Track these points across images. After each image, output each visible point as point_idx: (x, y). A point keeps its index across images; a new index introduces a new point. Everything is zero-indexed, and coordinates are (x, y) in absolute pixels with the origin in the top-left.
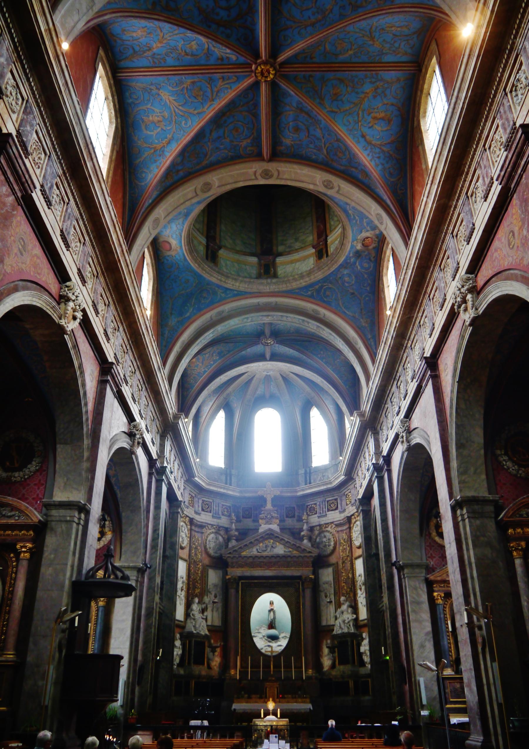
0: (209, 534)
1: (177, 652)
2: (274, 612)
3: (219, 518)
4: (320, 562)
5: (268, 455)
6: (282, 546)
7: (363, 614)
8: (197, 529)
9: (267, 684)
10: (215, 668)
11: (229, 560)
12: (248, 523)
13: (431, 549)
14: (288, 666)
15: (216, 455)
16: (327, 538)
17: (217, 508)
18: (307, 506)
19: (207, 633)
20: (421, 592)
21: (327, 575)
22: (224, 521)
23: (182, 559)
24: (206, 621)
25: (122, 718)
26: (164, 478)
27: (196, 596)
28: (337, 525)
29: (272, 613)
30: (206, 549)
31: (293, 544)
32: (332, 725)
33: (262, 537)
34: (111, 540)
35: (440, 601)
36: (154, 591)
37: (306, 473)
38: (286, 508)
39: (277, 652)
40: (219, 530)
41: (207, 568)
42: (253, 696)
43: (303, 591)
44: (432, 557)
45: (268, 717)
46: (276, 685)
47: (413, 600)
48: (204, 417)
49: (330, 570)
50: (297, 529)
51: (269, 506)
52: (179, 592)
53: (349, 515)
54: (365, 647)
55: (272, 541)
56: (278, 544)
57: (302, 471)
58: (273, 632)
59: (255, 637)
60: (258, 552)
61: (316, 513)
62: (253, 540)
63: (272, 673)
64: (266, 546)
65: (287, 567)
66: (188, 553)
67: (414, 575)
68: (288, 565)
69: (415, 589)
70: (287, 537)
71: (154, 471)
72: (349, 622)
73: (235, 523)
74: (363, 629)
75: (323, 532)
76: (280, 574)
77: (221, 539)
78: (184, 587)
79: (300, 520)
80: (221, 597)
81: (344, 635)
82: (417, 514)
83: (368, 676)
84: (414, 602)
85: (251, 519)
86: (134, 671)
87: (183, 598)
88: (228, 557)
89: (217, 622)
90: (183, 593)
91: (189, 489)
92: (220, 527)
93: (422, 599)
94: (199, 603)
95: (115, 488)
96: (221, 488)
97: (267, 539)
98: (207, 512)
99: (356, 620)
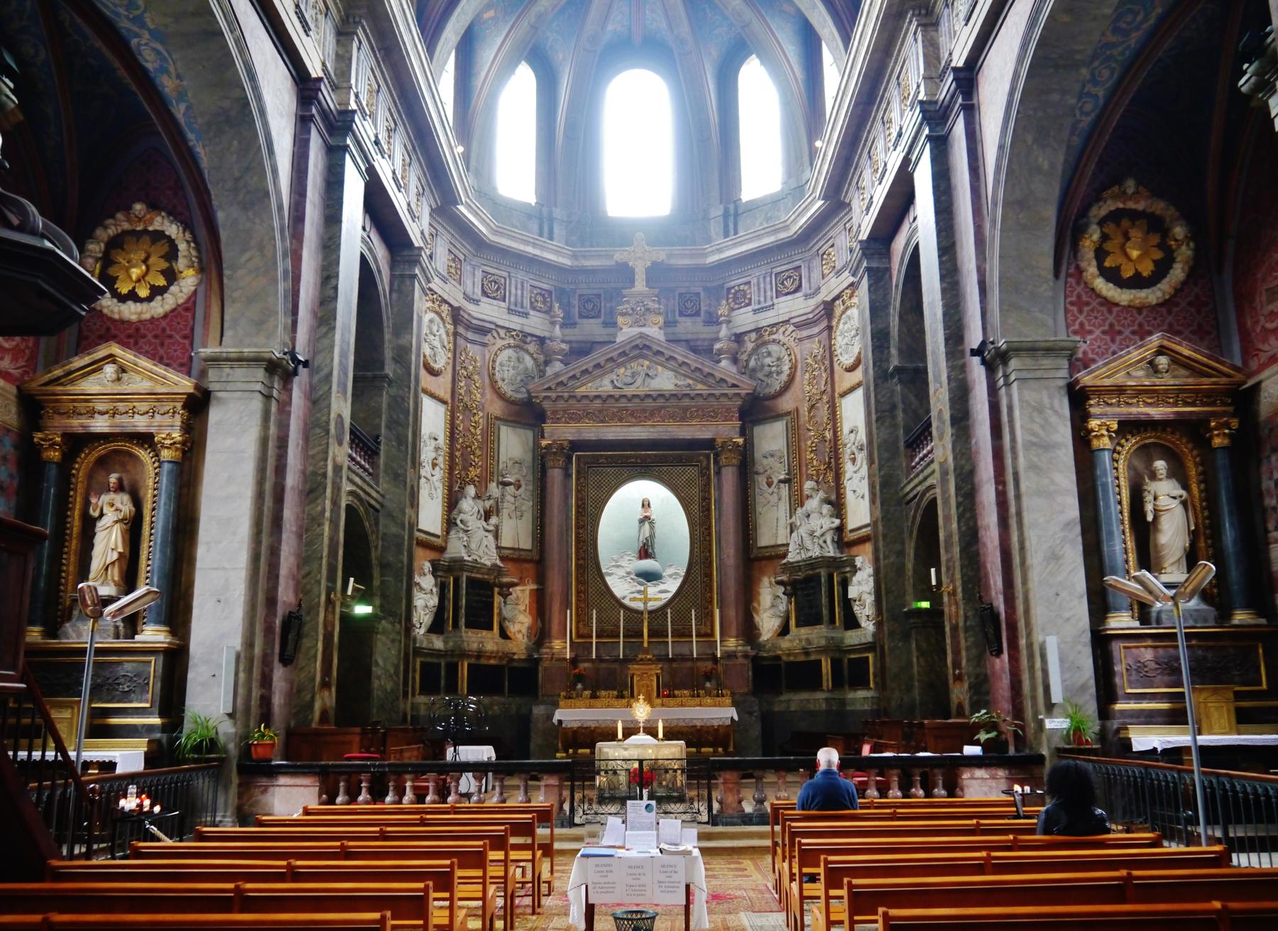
0: (500, 350)
1: (425, 601)
2: (652, 523)
3: (526, 315)
4: (755, 410)
5: (639, 174)
6: (671, 373)
7: (859, 513)
8: (470, 335)
9: (634, 668)
10: (520, 636)
11: (547, 405)
12: (592, 328)
13: (1081, 312)
14: (682, 633)
15: (515, 171)
16: (775, 355)
17: (519, 292)
18: (729, 289)
19: (498, 562)
20: (1053, 419)
22: (535, 323)
23: (433, 396)
24: (497, 537)
25: (231, 746)
26: (348, 142)
27: (472, 482)
28: (799, 326)
29: (647, 524)
30: (493, 383)
32: (829, 763)
33: (624, 354)
34: (195, 292)
35: (1106, 440)
36: (328, 432)
37: (726, 215)
38: (681, 295)
39: (656, 599)
42: (603, 693)
43: (718, 473)
44: (1082, 331)
45: (633, 737)
46: (656, 669)
47: (1034, 439)
50: (704, 340)
51: (640, 285)
52: (426, 471)
53: (829, 299)
54: (862, 586)
55: (647, 363)
56: (660, 368)
57: (717, 211)
58: (647, 564)
59: (610, 575)
60: (615, 387)
61: (749, 304)
62: (602, 361)
63: (646, 645)
64: (633, 375)
65: (683, 419)
66: (449, 386)
67: (1039, 374)
68: (683, 416)
69: (1040, 410)
70: (680, 353)
71: (314, 111)
72: (822, 535)
73: (561, 327)
74: (855, 550)
75: (765, 343)
76: (665, 436)
77: (529, 362)
78: (441, 459)
79: (713, 320)
80: (531, 488)
81: (812, 564)
82: (1051, 213)
83: (870, 647)
84: (1034, 444)
85: (599, 321)
86: (269, 630)
88: (545, 397)
89: (526, 543)
90: (439, 474)
91: (449, 237)
92: (526, 335)
93: (1057, 438)
94: (477, 497)
95: (191, 136)
96: (527, 243)
97: (636, 358)
99: (840, 530)
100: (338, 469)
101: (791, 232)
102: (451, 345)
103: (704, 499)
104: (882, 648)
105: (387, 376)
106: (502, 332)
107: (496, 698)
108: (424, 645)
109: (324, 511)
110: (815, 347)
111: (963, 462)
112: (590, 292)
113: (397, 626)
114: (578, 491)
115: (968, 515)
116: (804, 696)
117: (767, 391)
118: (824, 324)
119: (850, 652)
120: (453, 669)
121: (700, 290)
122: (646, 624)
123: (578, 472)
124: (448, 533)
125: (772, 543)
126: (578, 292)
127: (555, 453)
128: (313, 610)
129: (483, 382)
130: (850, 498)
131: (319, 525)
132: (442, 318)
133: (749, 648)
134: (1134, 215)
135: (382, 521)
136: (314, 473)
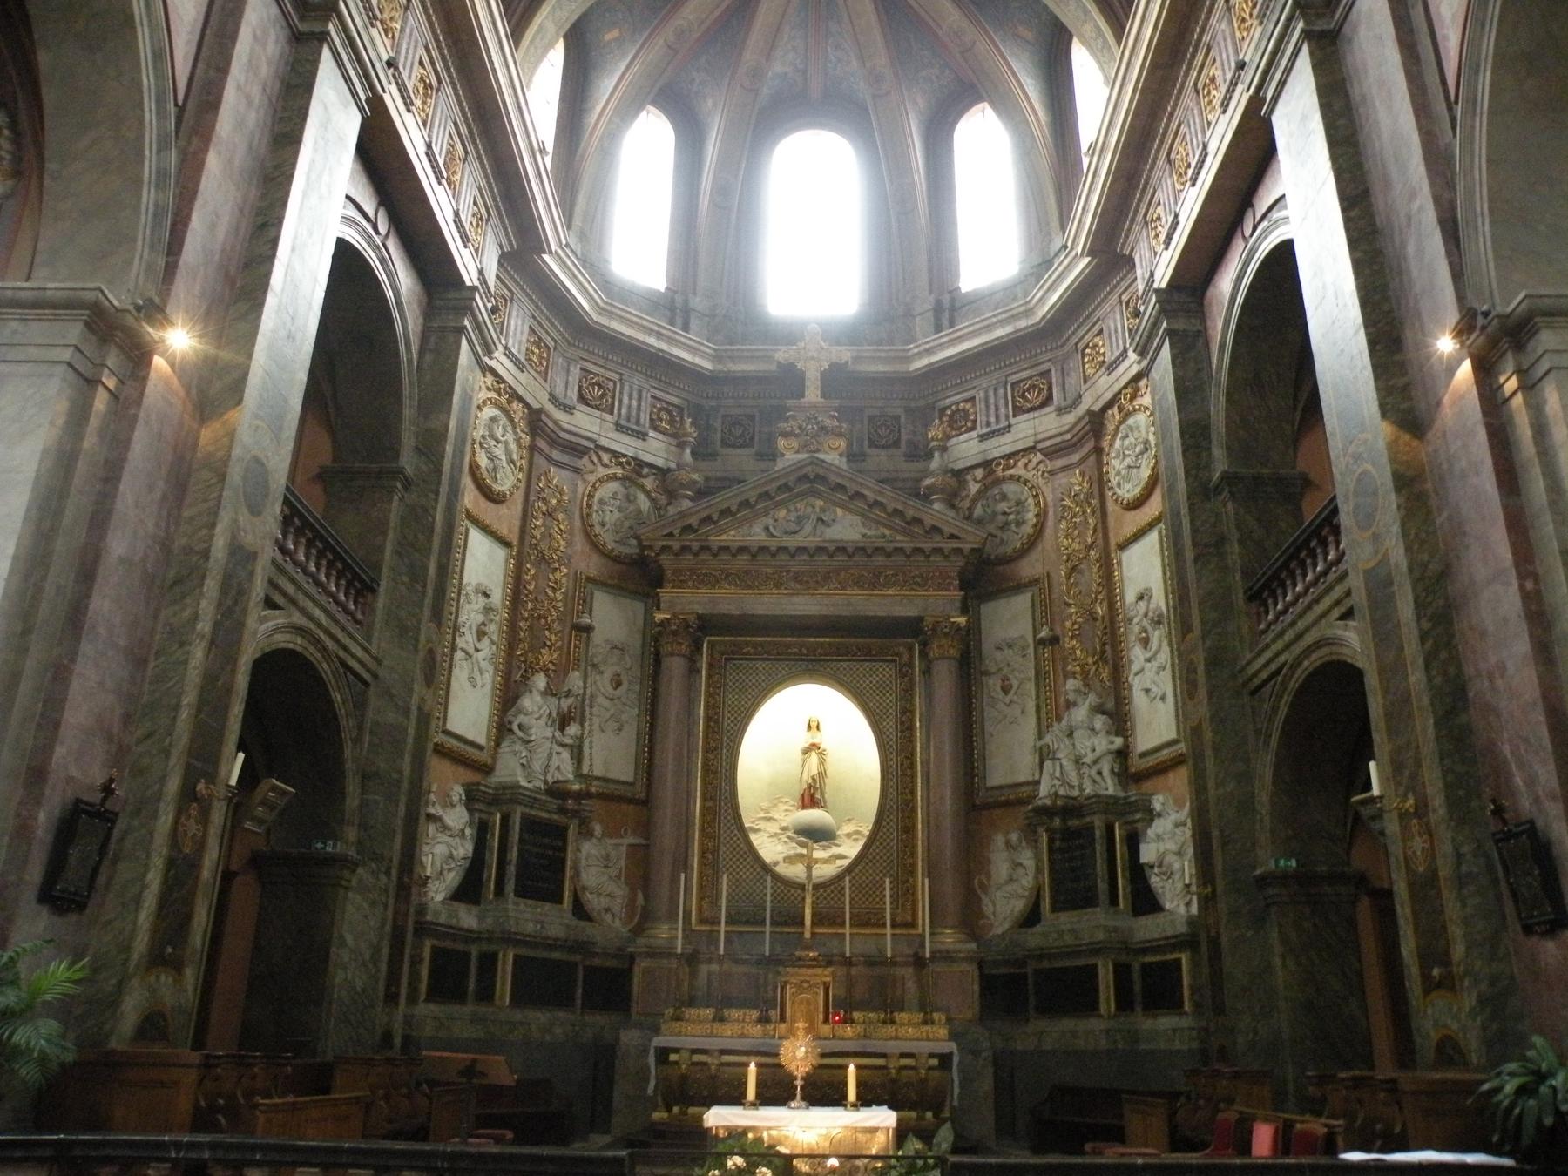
0: (601, 481)
2: (822, 754)
3: (643, 436)
4: (984, 577)
11: (666, 560)
17: (634, 403)
18: (942, 410)
21: (1010, 620)
22: (655, 450)
23: (486, 530)
28: (1050, 454)
29: (814, 756)
31: (896, 511)
33: (785, 487)
40: (640, 475)
41: (590, 586)
43: (927, 672)
48: (598, 109)
49: (1021, 603)
51: (813, 394)
52: (467, 640)
53: (1096, 408)
54: (1167, 842)
56: (840, 512)
57: (925, 304)
58: (814, 815)
59: (756, 831)
61: (973, 428)
62: (752, 496)
63: (807, 935)
64: (800, 520)
65: (874, 586)
66: (517, 523)
68: (874, 581)
72: (1096, 762)
74: (1148, 786)
75: (999, 482)
76: (845, 611)
77: (643, 502)
78: (492, 628)
80: (637, 688)
83: (1188, 942)
87: (489, 669)
88: (664, 548)
90: (486, 650)
91: (532, 307)
92: (641, 464)
94: (548, 692)
96: (650, 331)
97: (801, 495)
98: (597, 408)
99: (1122, 754)
100: (242, 556)
101: (1037, 318)
102: (524, 463)
103: (904, 712)
104: (1215, 943)
105: (401, 471)
106: (606, 458)
107: (561, 1014)
108: (443, 919)
109: (195, 617)
110: (1076, 481)
111: (1426, 557)
112: (738, 411)
113: (383, 877)
114: (709, 695)
115: (1443, 655)
116: (1067, 1024)
117: (1001, 550)
118: (1091, 444)
119: (1145, 951)
120: (489, 963)
121: (899, 411)
122: (808, 901)
123: (710, 666)
124: (498, 745)
125: (1009, 780)
126: (722, 411)
127: (674, 633)
128: (146, 807)
129: (571, 524)
130: (1139, 700)
131: (182, 644)
132: (511, 420)
133: (973, 946)
135: (374, 701)
136: (187, 550)
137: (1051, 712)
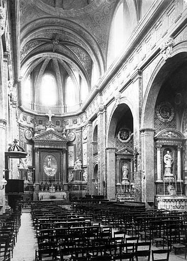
4: (69, 144)
21: (71, 149)
44: (117, 146)
49: (73, 147)
51: (50, 120)
54: (85, 174)
99: (82, 165)
130: (84, 161)
134: (125, 130)
137: (75, 160)
